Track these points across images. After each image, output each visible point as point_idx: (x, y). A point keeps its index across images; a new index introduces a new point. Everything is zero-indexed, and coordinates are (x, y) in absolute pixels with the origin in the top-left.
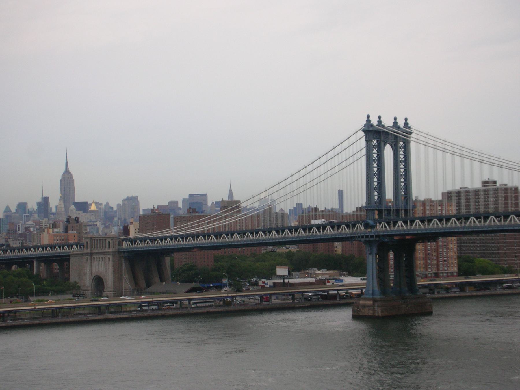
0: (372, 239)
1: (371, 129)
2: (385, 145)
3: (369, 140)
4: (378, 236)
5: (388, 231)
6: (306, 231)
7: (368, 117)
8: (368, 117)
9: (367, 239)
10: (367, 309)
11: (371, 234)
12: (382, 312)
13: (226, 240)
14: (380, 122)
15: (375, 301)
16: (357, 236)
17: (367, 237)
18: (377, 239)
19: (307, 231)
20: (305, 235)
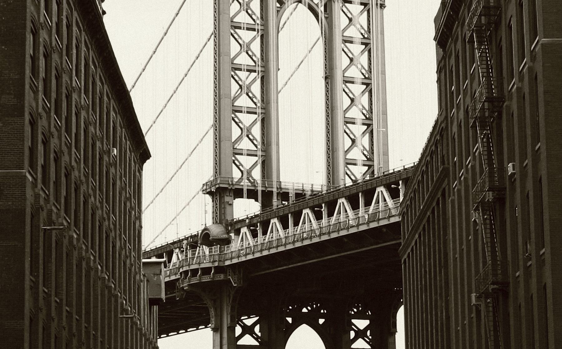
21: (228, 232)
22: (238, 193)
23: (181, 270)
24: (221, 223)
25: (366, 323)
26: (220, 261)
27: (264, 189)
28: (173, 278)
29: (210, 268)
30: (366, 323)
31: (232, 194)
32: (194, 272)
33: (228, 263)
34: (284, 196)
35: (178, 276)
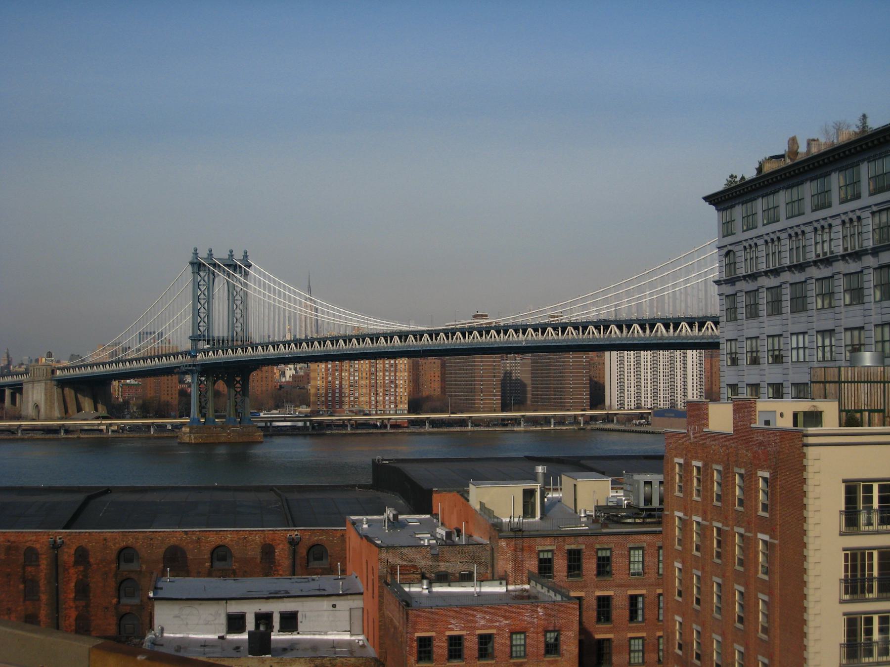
0: (190, 368)
1: (195, 261)
4: (194, 365)
5: (641, 337)
6: (669, 328)
7: (196, 250)
8: (196, 250)
9: (186, 368)
12: (195, 438)
13: (574, 337)
17: (186, 366)
19: (671, 327)
20: (643, 335)
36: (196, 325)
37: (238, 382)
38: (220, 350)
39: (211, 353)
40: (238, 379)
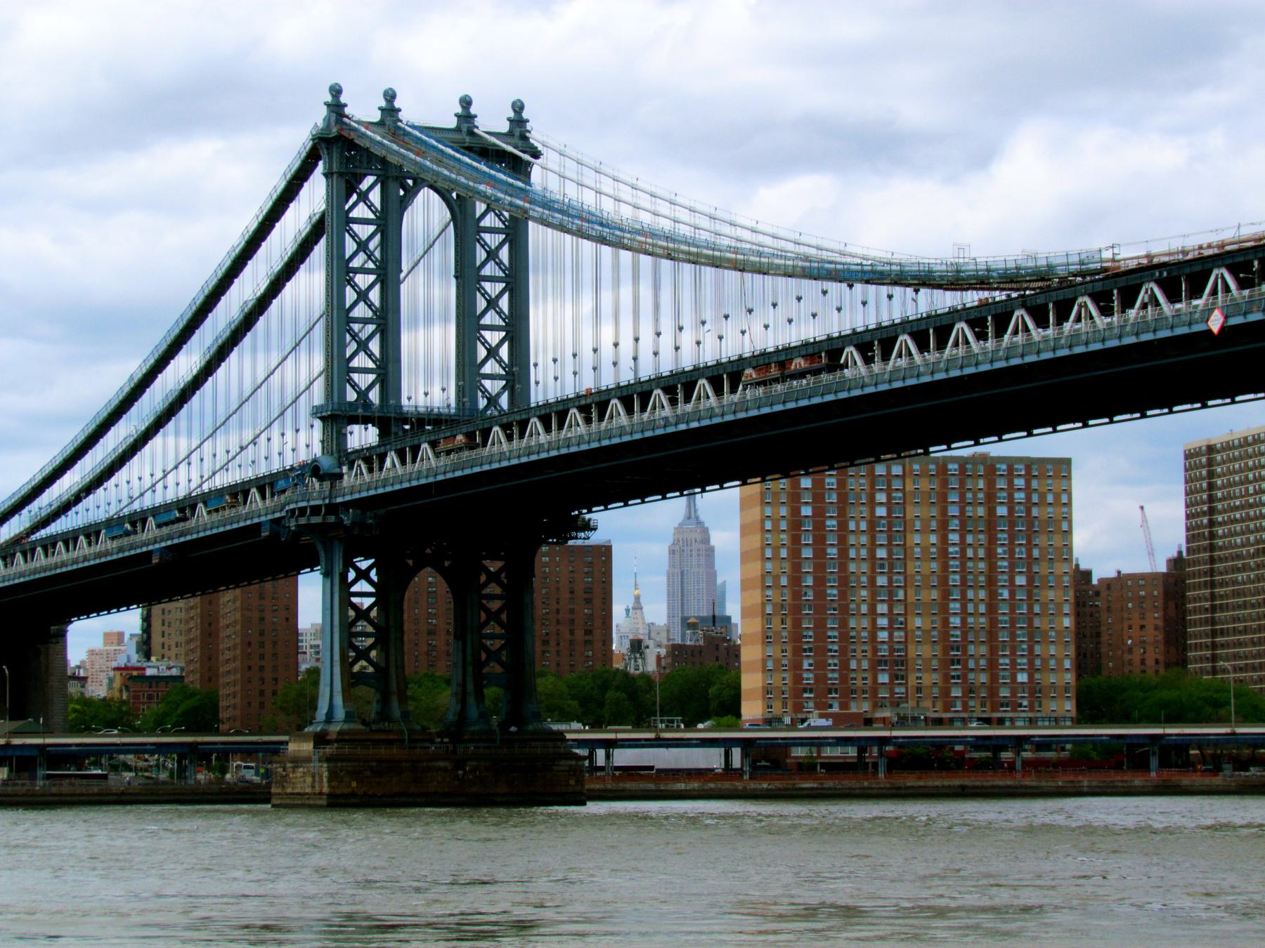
0: (316, 520)
2: (411, 193)
3: (332, 174)
7: (336, 91)
8: (336, 91)
9: (303, 521)
10: (301, 770)
11: (312, 503)
12: (333, 776)
14: (390, 111)
15: (320, 740)
16: (293, 511)
18: (332, 519)
21: (340, 465)
22: (354, 420)
23: (287, 508)
24: (332, 454)
25: (499, 564)
26: (330, 497)
27: (381, 414)
28: (277, 515)
29: (319, 507)
30: (499, 564)
31: (345, 421)
32: (302, 511)
33: (339, 500)
34: (405, 420)
35: (283, 514)
36: (338, 370)
37: (493, 577)
38: (425, 446)
39: (391, 459)
40: (493, 566)
